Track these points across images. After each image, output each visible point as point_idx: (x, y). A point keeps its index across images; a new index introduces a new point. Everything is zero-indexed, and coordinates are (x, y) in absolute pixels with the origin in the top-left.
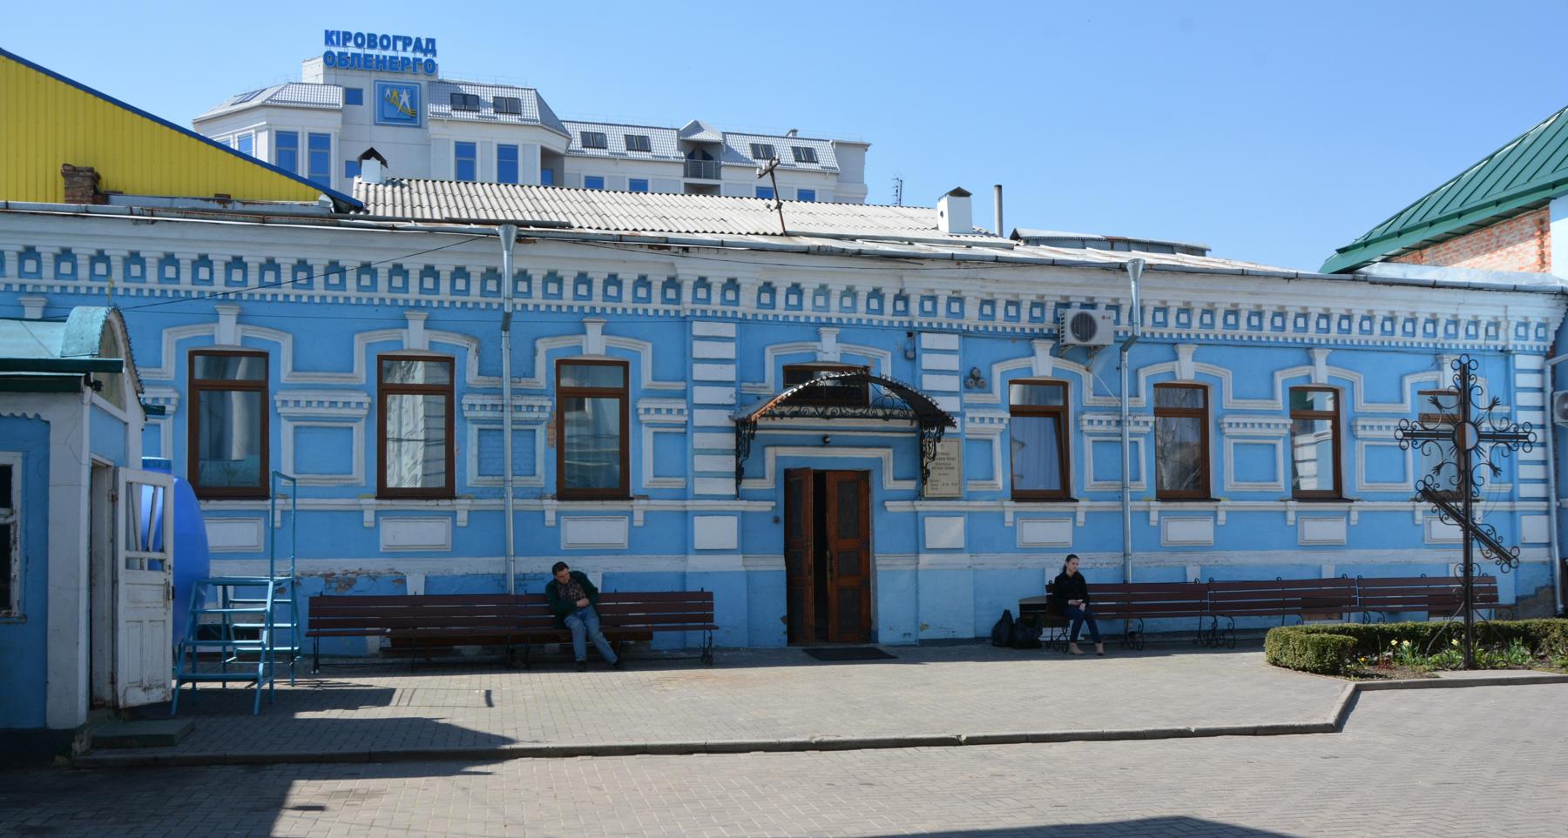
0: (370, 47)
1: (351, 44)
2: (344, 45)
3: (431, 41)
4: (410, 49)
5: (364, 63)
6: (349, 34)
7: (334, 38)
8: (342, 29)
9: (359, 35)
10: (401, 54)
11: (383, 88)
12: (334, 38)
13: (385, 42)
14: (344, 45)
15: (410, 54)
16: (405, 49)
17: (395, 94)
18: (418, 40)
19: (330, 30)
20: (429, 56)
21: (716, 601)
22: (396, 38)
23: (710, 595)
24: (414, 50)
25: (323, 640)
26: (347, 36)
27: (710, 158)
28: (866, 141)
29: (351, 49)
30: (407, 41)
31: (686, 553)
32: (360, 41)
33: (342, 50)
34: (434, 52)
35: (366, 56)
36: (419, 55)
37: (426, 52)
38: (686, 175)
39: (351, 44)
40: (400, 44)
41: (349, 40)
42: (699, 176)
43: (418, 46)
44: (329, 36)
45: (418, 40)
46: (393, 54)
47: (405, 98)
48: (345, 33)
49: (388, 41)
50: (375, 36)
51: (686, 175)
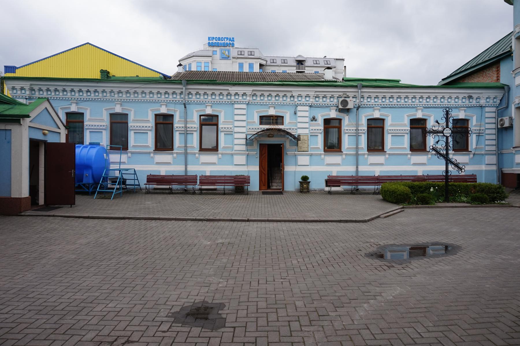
0: (219, 40)
1: (214, 40)
2: (213, 40)
3: (233, 38)
4: (228, 40)
5: (218, 45)
6: (214, 37)
7: (210, 39)
8: (212, 37)
9: (216, 38)
10: (226, 42)
11: (221, 51)
12: (210, 39)
13: (222, 39)
14: (213, 40)
15: (228, 42)
16: (227, 41)
17: (225, 51)
18: (230, 38)
19: (209, 37)
20: (233, 42)
21: (477, 177)
22: (225, 38)
23: (476, 175)
24: (229, 41)
25: (225, 186)
26: (213, 38)
27: (303, 64)
28: (344, 58)
29: (214, 41)
30: (227, 38)
31: (296, 165)
32: (216, 39)
33: (212, 41)
34: (234, 41)
35: (218, 43)
36: (230, 42)
37: (232, 41)
38: (296, 69)
39: (214, 40)
40: (226, 39)
41: (214, 39)
42: (300, 69)
43: (230, 40)
44: (209, 38)
45: (230, 38)
46: (224, 42)
47: (227, 52)
48: (213, 37)
49: (223, 39)
50: (220, 38)
51: (296, 69)
